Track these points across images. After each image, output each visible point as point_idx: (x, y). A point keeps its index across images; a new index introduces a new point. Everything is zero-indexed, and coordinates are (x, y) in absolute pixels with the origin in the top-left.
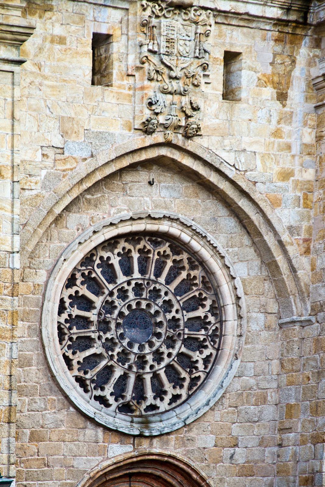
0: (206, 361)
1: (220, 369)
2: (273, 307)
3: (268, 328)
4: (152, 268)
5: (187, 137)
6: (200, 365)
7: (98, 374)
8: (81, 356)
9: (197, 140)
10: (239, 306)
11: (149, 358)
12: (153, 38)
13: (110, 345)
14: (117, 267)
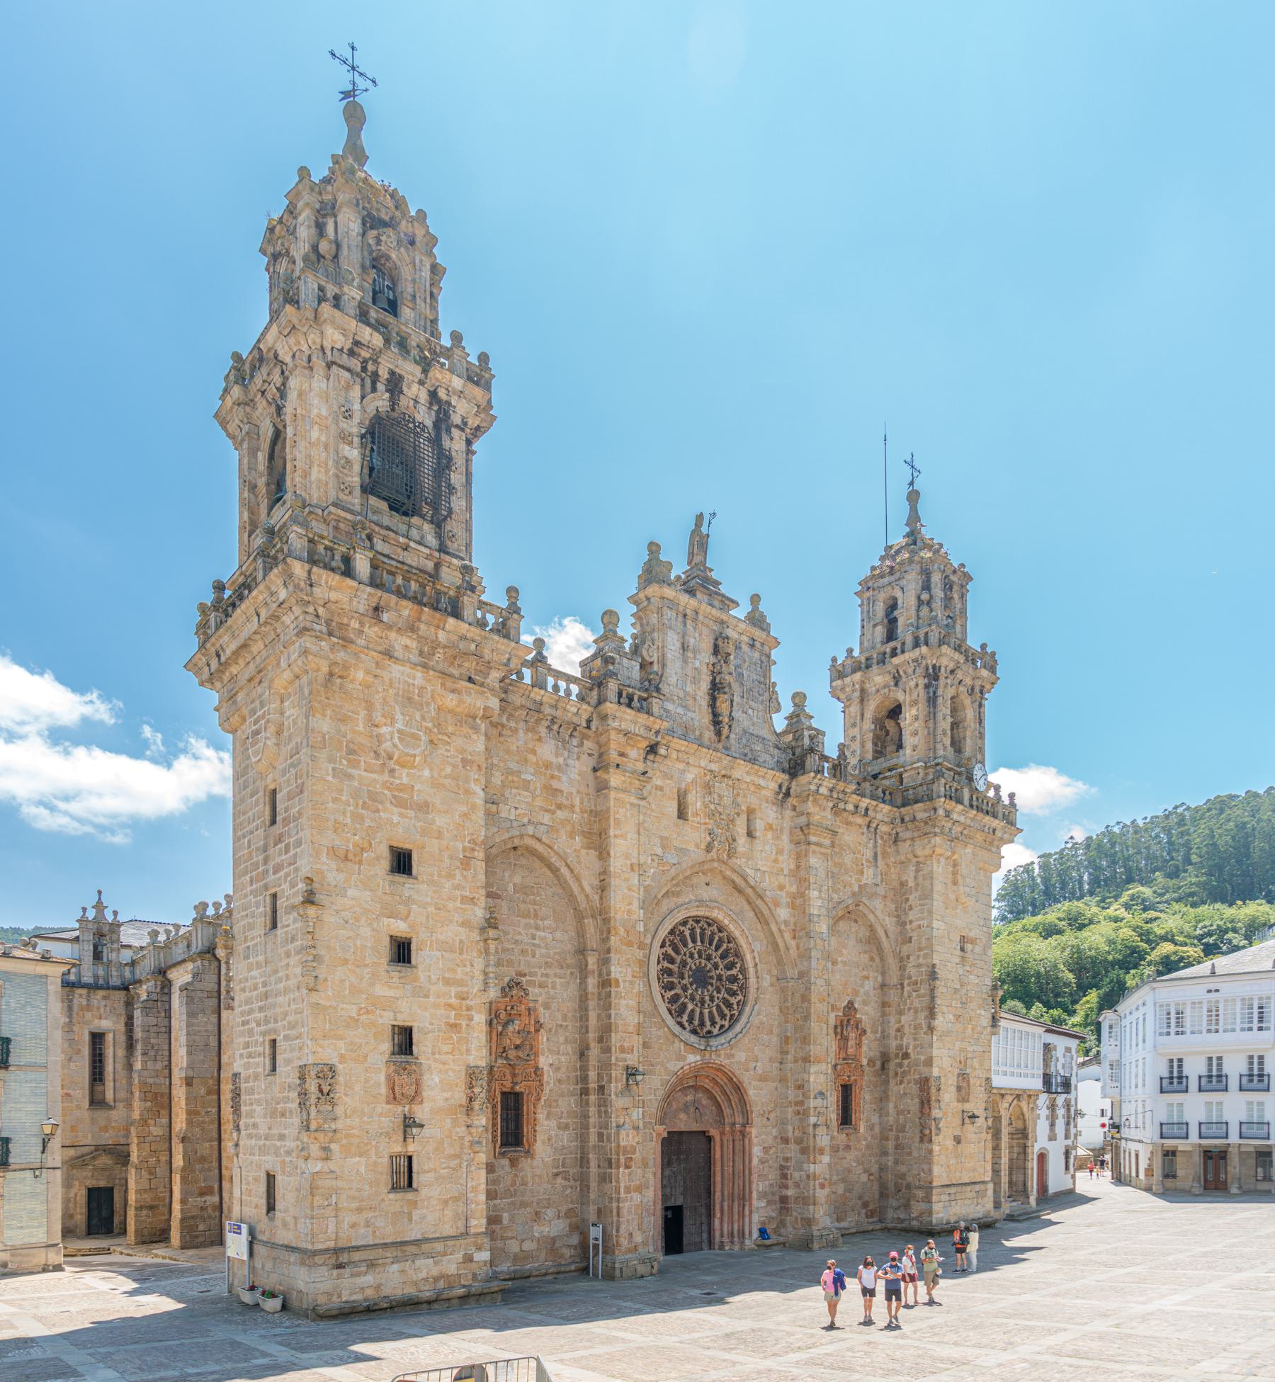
1: (747, 1009)
2: (775, 972)
3: (772, 985)
5: (729, 857)
8: (669, 994)
9: (734, 860)
11: (707, 998)
13: (685, 989)
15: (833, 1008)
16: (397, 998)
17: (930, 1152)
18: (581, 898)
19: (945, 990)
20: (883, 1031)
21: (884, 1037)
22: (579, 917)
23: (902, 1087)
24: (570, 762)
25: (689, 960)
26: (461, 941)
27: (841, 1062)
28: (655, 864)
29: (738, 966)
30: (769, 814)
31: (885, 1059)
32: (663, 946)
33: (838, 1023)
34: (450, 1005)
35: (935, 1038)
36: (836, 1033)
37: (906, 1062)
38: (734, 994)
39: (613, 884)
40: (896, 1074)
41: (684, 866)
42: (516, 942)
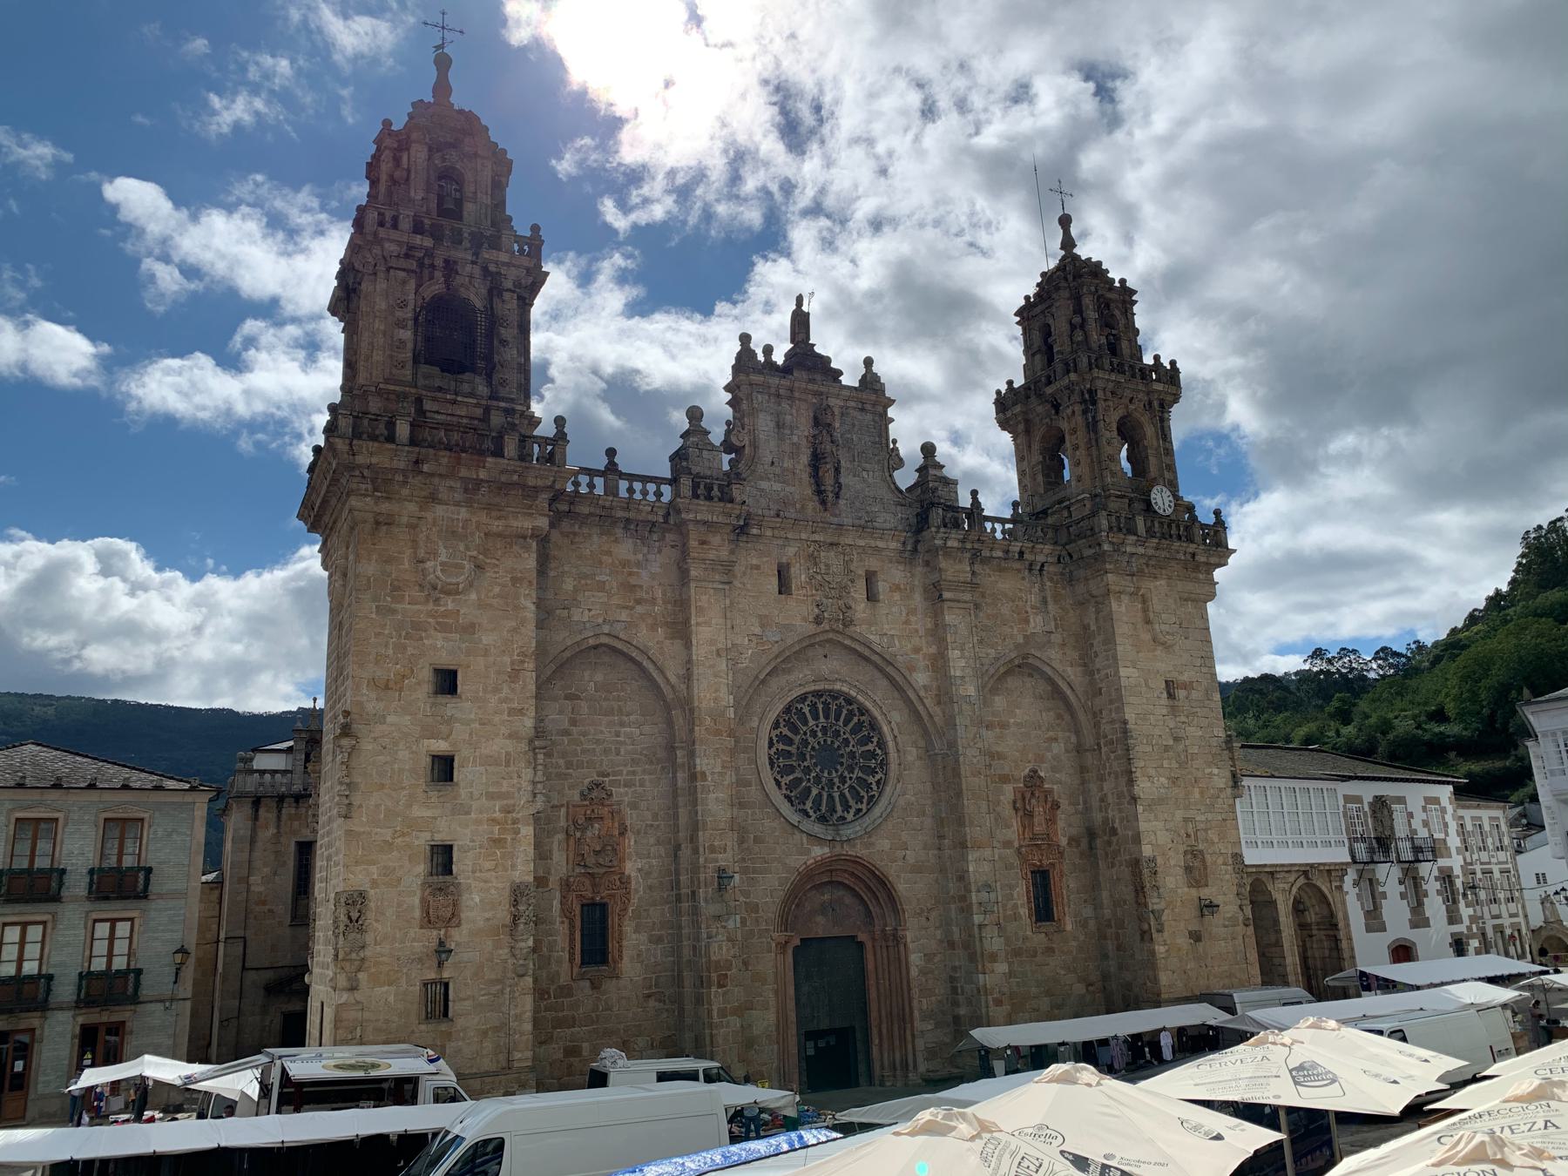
0: (878, 782)
1: (888, 789)
2: (922, 743)
4: (833, 715)
6: (874, 786)
7: (800, 793)
9: (852, 628)
10: (897, 744)
12: (816, 564)
14: (808, 715)
15: (1005, 779)
16: (435, 818)
17: (1153, 953)
18: (666, 689)
19: (1149, 749)
20: (1085, 802)
21: (1087, 809)
22: (668, 708)
23: (1114, 870)
24: (649, 557)
25: (811, 740)
26: (508, 754)
27: (1027, 842)
28: (753, 645)
29: (875, 740)
30: (893, 575)
31: (1091, 834)
32: (776, 725)
33: (1019, 796)
34: (493, 820)
35: (1140, 809)
36: (1016, 809)
37: (1114, 839)
38: (874, 772)
39: (696, 672)
40: (1107, 854)
41: (789, 642)
42: (598, 742)
